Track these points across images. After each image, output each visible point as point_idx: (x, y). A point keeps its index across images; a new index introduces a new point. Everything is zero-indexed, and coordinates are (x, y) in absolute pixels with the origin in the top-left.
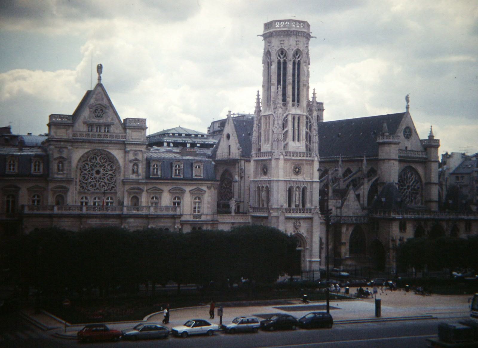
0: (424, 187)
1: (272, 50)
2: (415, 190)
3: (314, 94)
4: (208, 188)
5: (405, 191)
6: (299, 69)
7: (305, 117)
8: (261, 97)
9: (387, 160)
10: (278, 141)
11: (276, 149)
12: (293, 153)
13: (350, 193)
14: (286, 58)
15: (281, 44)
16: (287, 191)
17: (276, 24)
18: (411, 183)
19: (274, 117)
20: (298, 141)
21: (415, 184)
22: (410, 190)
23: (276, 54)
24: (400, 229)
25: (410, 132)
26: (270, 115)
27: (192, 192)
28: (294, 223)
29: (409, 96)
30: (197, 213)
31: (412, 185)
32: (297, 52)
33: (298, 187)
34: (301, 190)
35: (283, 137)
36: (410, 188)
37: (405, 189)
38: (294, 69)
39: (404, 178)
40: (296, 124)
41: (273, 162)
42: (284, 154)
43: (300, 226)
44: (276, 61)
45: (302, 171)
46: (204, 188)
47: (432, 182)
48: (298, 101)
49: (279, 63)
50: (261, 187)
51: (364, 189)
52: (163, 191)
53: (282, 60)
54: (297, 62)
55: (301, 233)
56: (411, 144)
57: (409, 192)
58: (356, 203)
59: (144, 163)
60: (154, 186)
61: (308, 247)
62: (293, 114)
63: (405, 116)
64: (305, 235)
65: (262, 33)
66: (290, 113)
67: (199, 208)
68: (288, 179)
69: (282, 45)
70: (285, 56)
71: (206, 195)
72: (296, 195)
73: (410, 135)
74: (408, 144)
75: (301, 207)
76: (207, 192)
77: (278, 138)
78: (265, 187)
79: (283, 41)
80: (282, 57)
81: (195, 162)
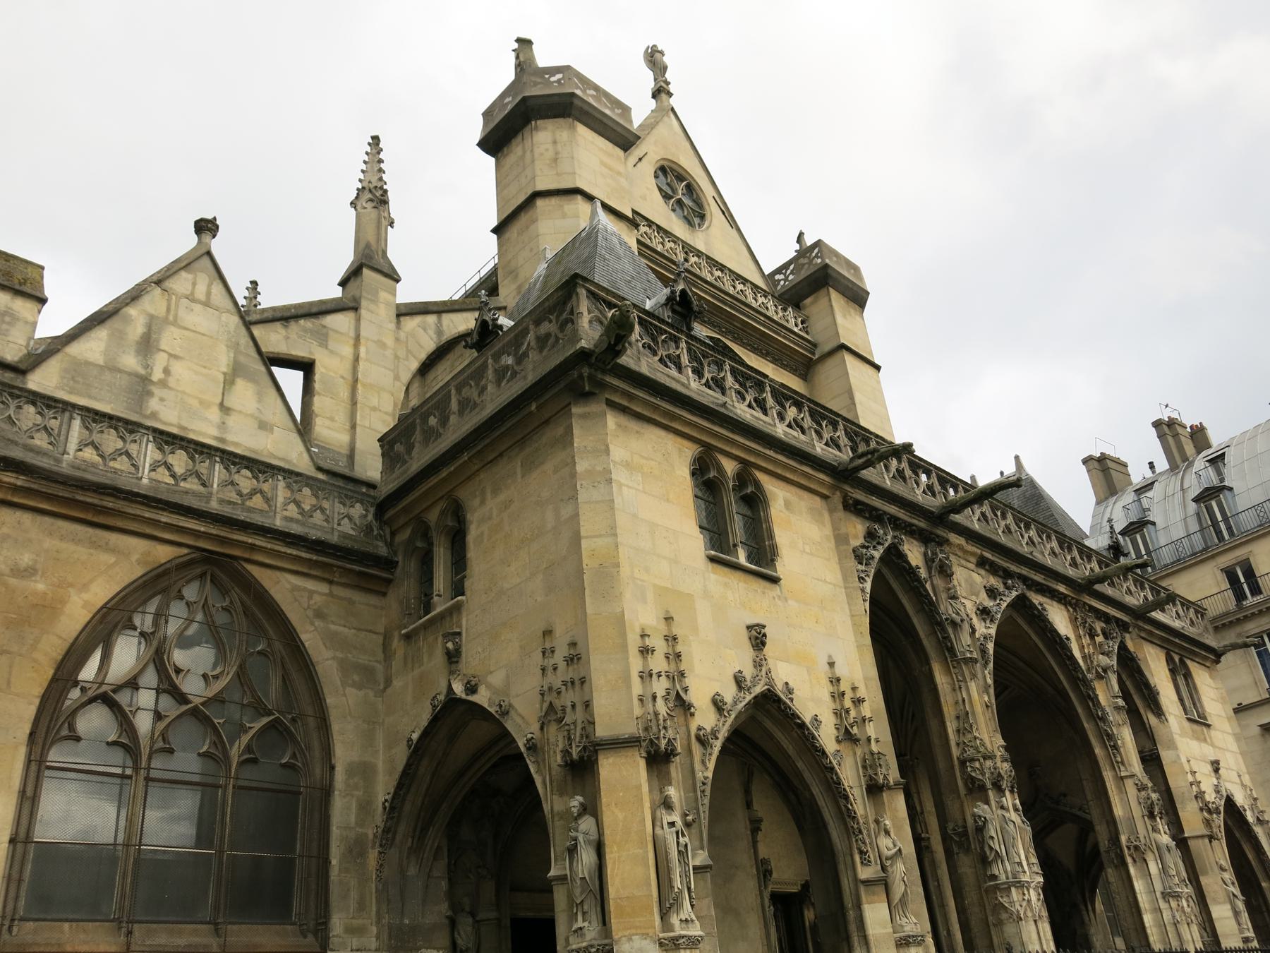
9: (554, 201)
51: (357, 338)
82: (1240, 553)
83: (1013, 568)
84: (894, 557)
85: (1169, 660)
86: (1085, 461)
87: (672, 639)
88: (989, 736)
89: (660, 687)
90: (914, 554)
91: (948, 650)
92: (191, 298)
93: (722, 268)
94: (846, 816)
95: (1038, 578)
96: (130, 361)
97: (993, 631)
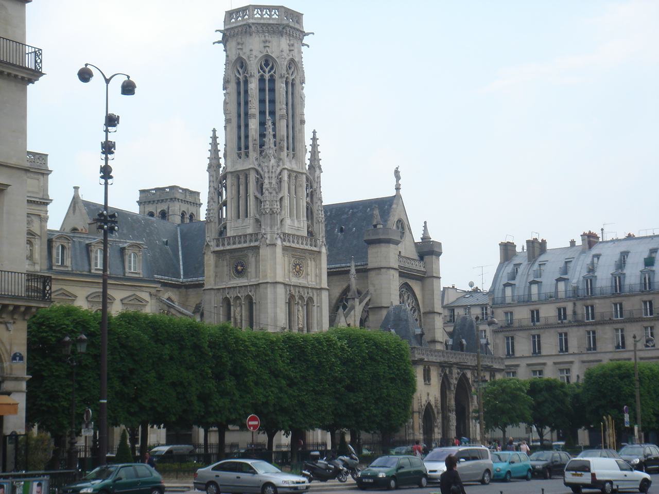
0: (422, 320)
1: (249, 58)
3: (314, 139)
4: (151, 295)
8: (221, 141)
9: (385, 270)
10: (271, 214)
11: (268, 229)
12: (293, 235)
13: (341, 321)
14: (275, 73)
15: (265, 47)
16: (286, 303)
17: (255, 12)
19: (257, 172)
23: (257, 64)
24: (425, 381)
25: (403, 226)
26: (249, 169)
27: (125, 302)
29: (399, 170)
33: (301, 298)
34: (305, 303)
35: (279, 207)
40: (293, 188)
41: (264, 252)
42: (282, 236)
44: (257, 76)
46: (145, 296)
47: (436, 311)
49: (262, 80)
50: (232, 301)
51: (355, 315)
52: (77, 297)
53: (267, 76)
59: (45, 240)
60: (60, 287)
63: (395, 201)
65: (223, 29)
66: (286, 167)
68: (287, 281)
69: (267, 48)
70: (272, 68)
72: (298, 311)
76: (149, 304)
77: (271, 209)
78: (243, 299)
81: (129, 246)
82: (537, 307)
83: (462, 367)
84: (445, 374)
85: (491, 374)
86: (500, 244)
87: (421, 397)
88: (453, 403)
89: (420, 404)
90: (447, 373)
91: (450, 388)
93: (409, 258)
94: (434, 417)
95: (467, 367)
97: (456, 383)
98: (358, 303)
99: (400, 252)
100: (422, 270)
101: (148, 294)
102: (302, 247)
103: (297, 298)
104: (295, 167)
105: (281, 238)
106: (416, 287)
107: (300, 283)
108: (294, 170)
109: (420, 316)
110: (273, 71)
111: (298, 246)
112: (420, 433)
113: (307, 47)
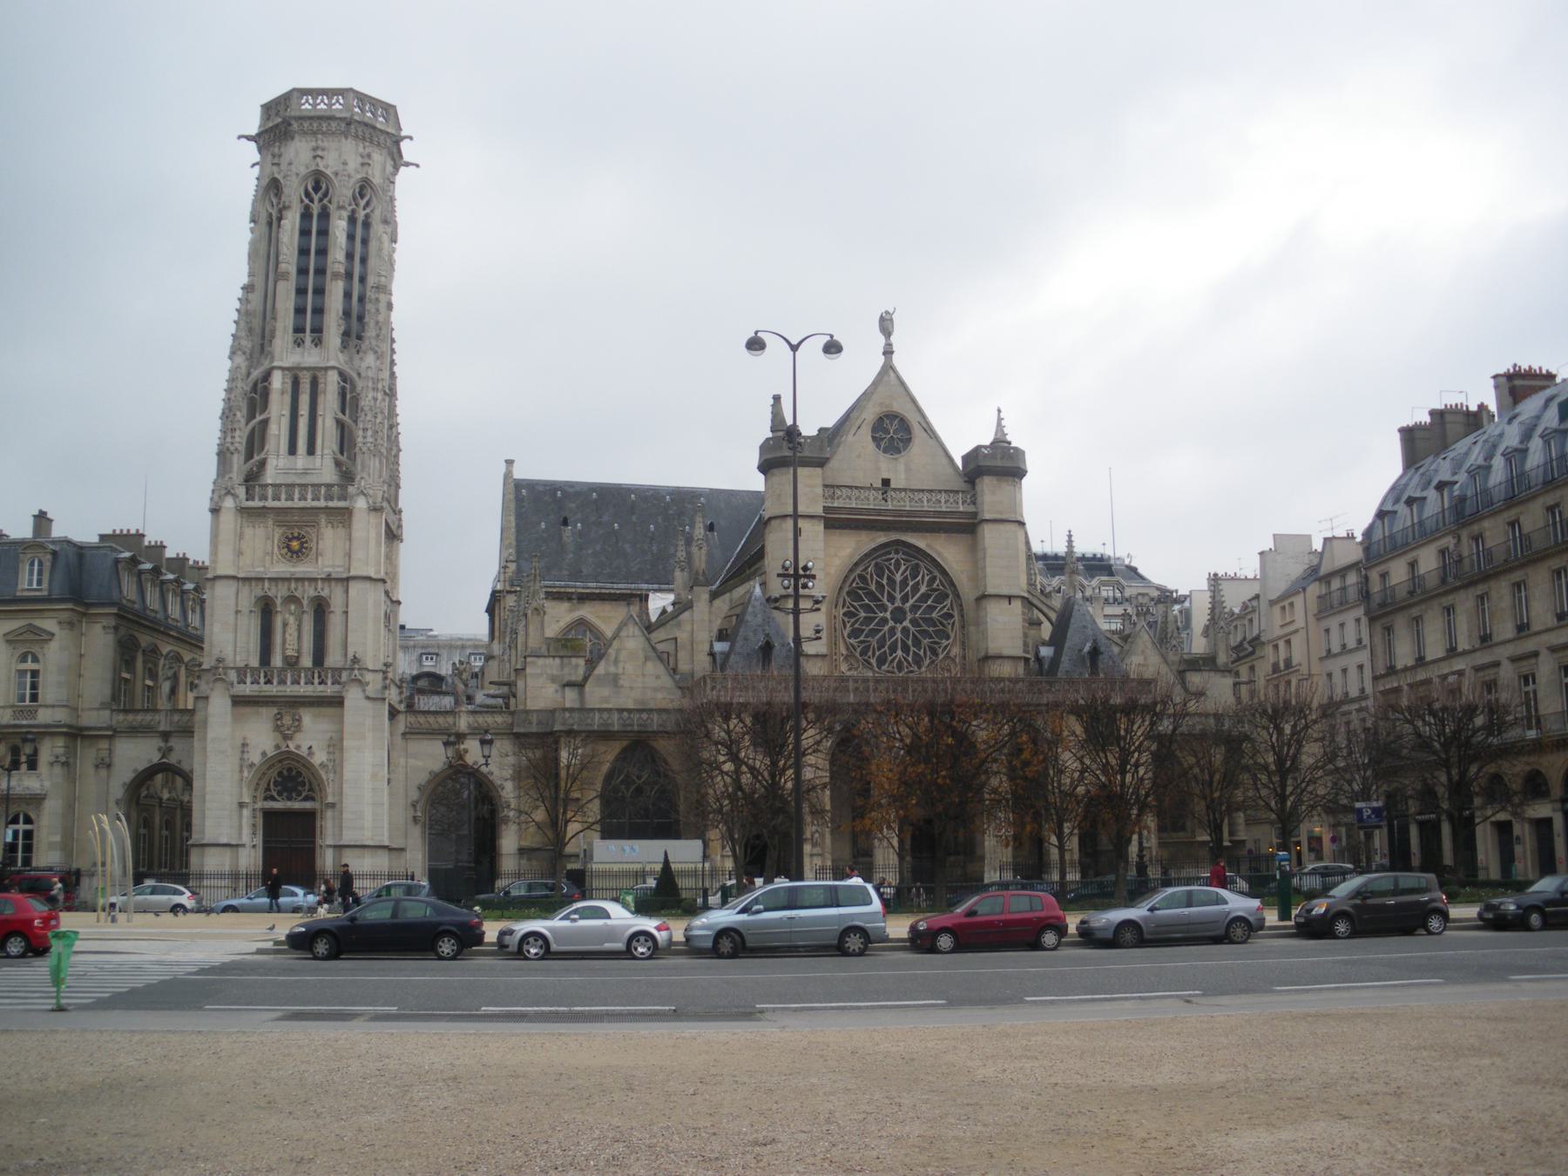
2: (931, 622)
4: (60, 623)
5: (886, 628)
6: (324, 233)
7: (333, 377)
16: (251, 611)
18: (911, 602)
20: (311, 451)
21: (929, 603)
22: (906, 623)
27: (10, 637)
28: (278, 717)
30: (27, 703)
31: (915, 608)
32: (318, 183)
36: (909, 616)
37: (884, 621)
38: (305, 233)
39: (880, 586)
40: (304, 399)
43: (298, 729)
44: (263, 219)
45: (314, 548)
46: (49, 624)
47: (990, 591)
48: (318, 330)
54: (316, 209)
55: (304, 752)
56: (908, 470)
57: (905, 631)
58: (654, 668)
61: (330, 799)
62: (288, 369)
64: (319, 758)
66: (276, 364)
67: (34, 686)
68: (259, 570)
69: (275, 169)
71: (54, 645)
72: (285, 625)
73: (908, 441)
74: (898, 471)
75: (307, 662)
76: (56, 637)
79: (280, 156)
80: (275, 201)
92: (628, 637)
96: (612, 669)
98: (706, 596)
99: (886, 482)
100: (961, 509)
101: (55, 621)
102: (302, 504)
103: (279, 602)
104: (310, 357)
105: (235, 496)
106: (948, 552)
107: (293, 573)
108: (302, 365)
109: (961, 605)
110: (327, 199)
111: (289, 504)
112: (722, 856)
113: (408, 140)
